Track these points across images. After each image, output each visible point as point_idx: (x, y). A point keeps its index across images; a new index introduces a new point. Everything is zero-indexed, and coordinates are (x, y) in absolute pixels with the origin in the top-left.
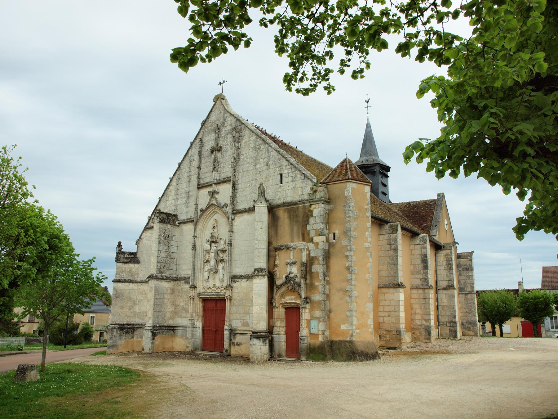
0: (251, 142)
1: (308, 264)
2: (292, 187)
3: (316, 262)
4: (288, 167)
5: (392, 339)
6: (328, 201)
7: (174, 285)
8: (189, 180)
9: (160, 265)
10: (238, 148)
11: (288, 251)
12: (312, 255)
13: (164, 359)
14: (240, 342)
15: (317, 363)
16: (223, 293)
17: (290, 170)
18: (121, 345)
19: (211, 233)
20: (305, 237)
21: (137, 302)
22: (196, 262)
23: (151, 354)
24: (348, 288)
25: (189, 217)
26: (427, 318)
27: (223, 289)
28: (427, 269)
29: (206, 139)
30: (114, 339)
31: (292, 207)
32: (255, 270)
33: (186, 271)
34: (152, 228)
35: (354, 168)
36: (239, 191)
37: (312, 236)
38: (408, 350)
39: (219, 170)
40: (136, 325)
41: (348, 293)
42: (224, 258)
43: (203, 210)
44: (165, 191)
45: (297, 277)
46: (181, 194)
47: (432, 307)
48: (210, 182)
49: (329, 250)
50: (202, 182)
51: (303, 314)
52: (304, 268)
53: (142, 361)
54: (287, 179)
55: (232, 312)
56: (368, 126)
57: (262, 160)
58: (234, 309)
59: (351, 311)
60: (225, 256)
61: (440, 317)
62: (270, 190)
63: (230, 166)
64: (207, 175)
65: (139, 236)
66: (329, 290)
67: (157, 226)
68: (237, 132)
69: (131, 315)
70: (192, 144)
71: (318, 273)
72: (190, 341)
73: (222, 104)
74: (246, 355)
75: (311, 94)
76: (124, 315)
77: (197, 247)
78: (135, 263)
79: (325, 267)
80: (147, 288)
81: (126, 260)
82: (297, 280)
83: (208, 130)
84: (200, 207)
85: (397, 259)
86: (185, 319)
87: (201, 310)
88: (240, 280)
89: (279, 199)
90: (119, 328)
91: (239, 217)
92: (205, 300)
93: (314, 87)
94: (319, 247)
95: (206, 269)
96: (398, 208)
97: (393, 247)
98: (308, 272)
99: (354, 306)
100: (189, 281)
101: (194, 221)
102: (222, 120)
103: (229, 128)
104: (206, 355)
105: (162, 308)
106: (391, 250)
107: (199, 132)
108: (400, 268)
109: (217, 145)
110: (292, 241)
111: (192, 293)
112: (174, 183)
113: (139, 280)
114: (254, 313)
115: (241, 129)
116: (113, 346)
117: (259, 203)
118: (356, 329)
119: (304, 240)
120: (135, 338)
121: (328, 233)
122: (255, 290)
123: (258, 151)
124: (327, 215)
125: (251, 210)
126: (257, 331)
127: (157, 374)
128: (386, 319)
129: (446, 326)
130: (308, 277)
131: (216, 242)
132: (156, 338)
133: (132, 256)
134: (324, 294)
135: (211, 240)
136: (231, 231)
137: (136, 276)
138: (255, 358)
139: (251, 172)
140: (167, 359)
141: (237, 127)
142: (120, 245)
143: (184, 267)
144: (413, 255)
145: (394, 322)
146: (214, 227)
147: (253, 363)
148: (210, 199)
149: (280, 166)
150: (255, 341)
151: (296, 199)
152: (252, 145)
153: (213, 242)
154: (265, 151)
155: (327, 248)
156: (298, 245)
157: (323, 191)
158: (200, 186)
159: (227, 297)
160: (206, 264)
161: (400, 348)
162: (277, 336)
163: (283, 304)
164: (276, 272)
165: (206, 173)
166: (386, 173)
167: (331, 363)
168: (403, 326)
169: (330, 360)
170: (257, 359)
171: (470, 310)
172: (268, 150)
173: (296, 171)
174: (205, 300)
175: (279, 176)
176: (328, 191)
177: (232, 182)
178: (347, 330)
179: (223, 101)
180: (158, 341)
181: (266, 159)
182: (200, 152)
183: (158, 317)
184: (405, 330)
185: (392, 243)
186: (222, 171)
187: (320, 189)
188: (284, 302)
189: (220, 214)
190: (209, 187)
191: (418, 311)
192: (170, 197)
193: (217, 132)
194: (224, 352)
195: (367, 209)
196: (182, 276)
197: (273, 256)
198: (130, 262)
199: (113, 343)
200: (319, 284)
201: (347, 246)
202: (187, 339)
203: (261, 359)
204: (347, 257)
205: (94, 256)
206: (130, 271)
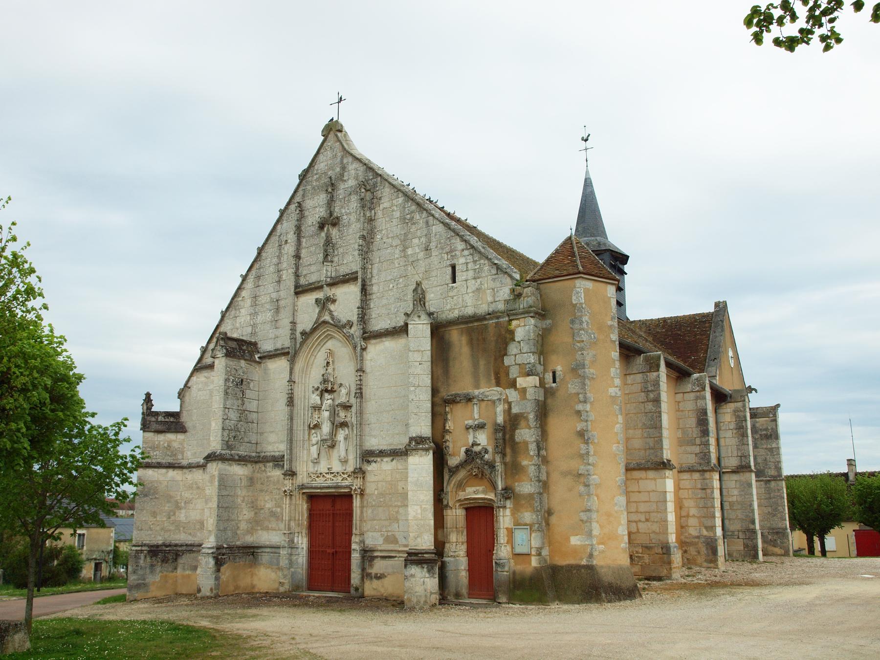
0: (395, 208)
1: (508, 428)
2: (474, 288)
3: (523, 423)
4: (466, 252)
5: (653, 562)
6: (542, 313)
7: (254, 471)
9: (229, 435)
10: (371, 220)
11: (470, 403)
12: (515, 410)
13: (244, 607)
14: (381, 572)
15: (530, 607)
16: (346, 483)
17: (470, 257)
18: (154, 583)
19: (323, 375)
20: (502, 378)
21: (183, 504)
22: (295, 428)
23: (215, 597)
24: (582, 469)
25: (279, 346)
26: (709, 524)
27: (346, 476)
28: (708, 435)
29: (309, 204)
30: (140, 572)
31: (476, 324)
32: (411, 439)
33: (275, 444)
34: (211, 367)
35: (587, 253)
36: (374, 296)
37: (515, 376)
38: (683, 581)
39: (336, 259)
40: (182, 546)
41: (582, 479)
43: (306, 333)
44: (233, 299)
45: (486, 452)
46: (262, 305)
47: (717, 504)
48: (319, 282)
49: (545, 402)
50: (303, 281)
51: (501, 518)
52: (501, 434)
53: (204, 612)
54: (465, 273)
55: (365, 518)
56: (588, 183)
57: (416, 241)
58: (369, 512)
59: (589, 510)
61: (727, 522)
62: (432, 295)
63: (356, 253)
64: (313, 268)
65: (184, 382)
66: (548, 474)
67: (221, 363)
68: (367, 191)
69: (172, 528)
70: (282, 213)
71: (526, 443)
72: (286, 572)
73: (339, 141)
74: (393, 596)
75: (801, 48)
76: (158, 528)
77: (295, 401)
78: (177, 431)
79: (540, 433)
80: (200, 477)
81: (160, 427)
82: (486, 456)
83: (314, 188)
84: (300, 328)
85: (660, 417)
86: (274, 532)
87: (306, 515)
88: (379, 459)
89: (450, 310)
90: (149, 552)
91: (375, 344)
92: (313, 499)
93: (805, 34)
94: (528, 396)
95: (314, 440)
96: (644, 330)
97: (652, 396)
98: (507, 442)
99: (594, 502)
100: (281, 463)
101: (289, 354)
102: (338, 169)
103: (352, 183)
104: (318, 597)
105: (233, 514)
106: (648, 401)
107: (296, 192)
108: (665, 433)
109: (331, 214)
110: (477, 387)
111: (288, 485)
112: (249, 284)
113: (185, 462)
114: (410, 518)
115: (375, 186)
116: (138, 587)
117: (416, 319)
118: (599, 544)
119: (498, 384)
120: (179, 571)
121: (542, 371)
122: (412, 476)
123: (409, 224)
124: (540, 338)
125: (402, 330)
126: (416, 551)
127: (245, 633)
128: (641, 525)
129: (738, 538)
130: (508, 450)
131: (331, 391)
132: (223, 569)
133: (172, 419)
134: (539, 481)
135: (322, 387)
136: (361, 370)
137: (180, 457)
138: (414, 600)
139: (396, 262)
140: (249, 607)
141: (367, 181)
142: (148, 399)
143: (272, 438)
144: (682, 411)
145: (658, 531)
146: (328, 363)
147: (412, 609)
148: (320, 312)
149: (451, 251)
150: (414, 570)
151: (483, 309)
152: (397, 214)
153: (327, 391)
154: (421, 223)
155: (542, 398)
156: (488, 393)
157: (533, 294)
158: (300, 289)
159: (355, 490)
160: (313, 431)
161: (669, 577)
162: (452, 559)
163: (462, 501)
164: (447, 444)
165: (310, 265)
166: (621, 266)
167: (554, 606)
168: (672, 539)
169: (553, 601)
170: (418, 602)
171: (776, 510)
172: (427, 223)
173: (480, 259)
174: (313, 499)
175: (450, 268)
176: (541, 296)
177: (360, 280)
178: (581, 546)
179: (339, 134)
181: (423, 239)
182: (298, 230)
183: (225, 529)
184: (677, 545)
185: (650, 389)
186: (341, 262)
187: (528, 291)
188: (463, 498)
189: (338, 339)
190: (317, 291)
191: (693, 511)
192: (243, 311)
193: (330, 190)
194: (352, 591)
195: (611, 326)
196: (268, 454)
197: (441, 415)
198: (168, 431)
199: (139, 579)
200: (528, 462)
201: (578, 394)
202: (280, 569)
203: (426, 602)
204: (579, 413)
205: (125, 416)
206: (168, 446)
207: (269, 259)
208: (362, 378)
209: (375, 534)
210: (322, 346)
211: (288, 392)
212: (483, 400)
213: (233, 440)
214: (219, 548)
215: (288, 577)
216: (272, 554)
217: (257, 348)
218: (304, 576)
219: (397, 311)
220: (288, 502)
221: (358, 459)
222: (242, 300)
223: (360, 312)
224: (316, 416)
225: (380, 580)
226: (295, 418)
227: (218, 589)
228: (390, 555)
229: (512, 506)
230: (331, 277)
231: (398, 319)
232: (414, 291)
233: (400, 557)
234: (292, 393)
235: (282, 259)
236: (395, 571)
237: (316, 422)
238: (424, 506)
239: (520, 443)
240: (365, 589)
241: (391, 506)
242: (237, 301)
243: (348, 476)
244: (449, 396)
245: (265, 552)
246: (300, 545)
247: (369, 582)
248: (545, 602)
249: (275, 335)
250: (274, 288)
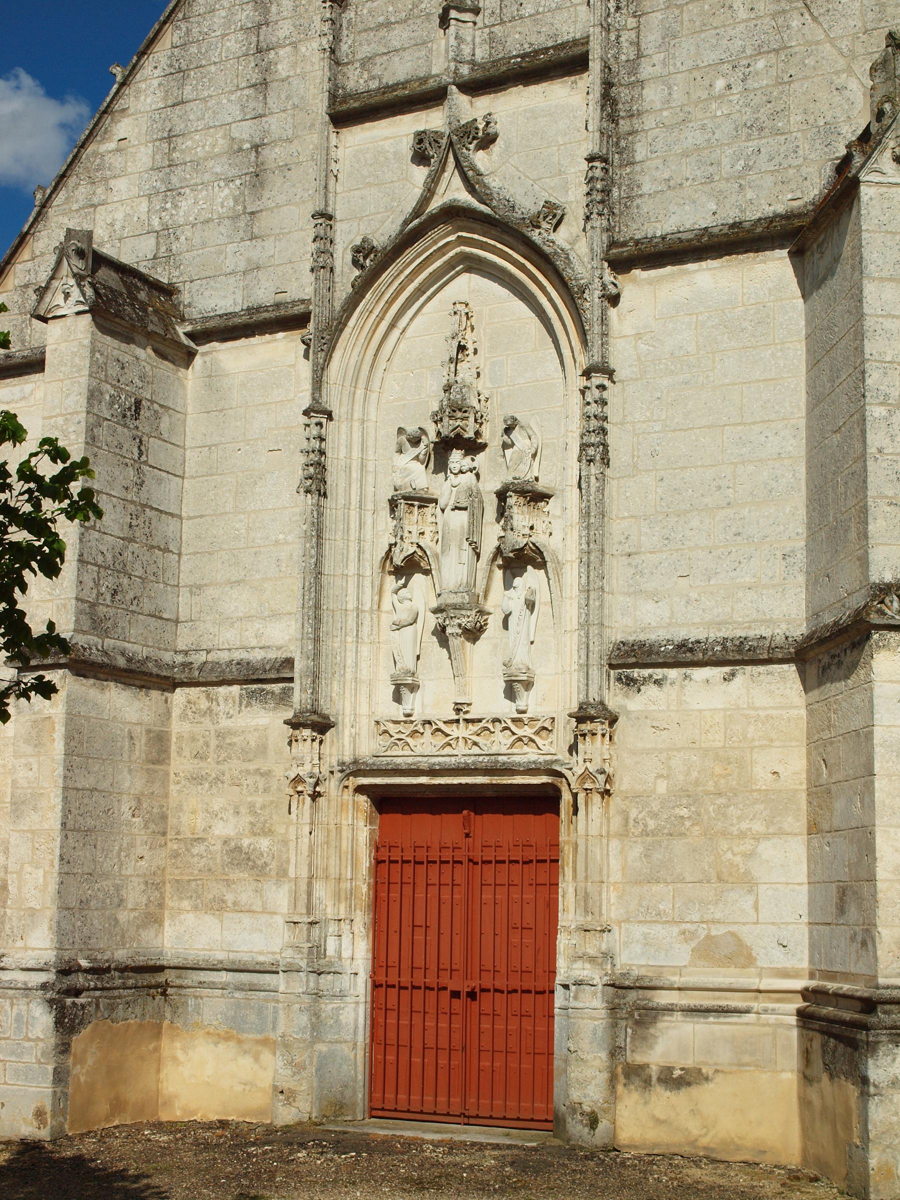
8: (255, 78)
9: (97, 584)
14: (689, 1063)
19: (448, 388)
27: (527, 731)
36: (649, 122)
42: (539, 538)
48: (424, 80)
60: (539, 526)
64: (398, 36)
74: (738, 1148)
86: (246, 919)
87: (365, 861)
100: (277, 687)
132: (78, 1041)
146: (461, 348)
165: (388, 25)
177: (595, 66)
180: (90, 1062)
192: (120, 185)
196: (224, 657)
207: (223, 13)
208: (605, 394)
209: (658, 931)
210: (430, 298)
211: (305, 445)
213: (108, 602)
214: (66, 970)
215: (304, 1074)
216: (237, 995)
217: (175, 307)
218: (360, 1068)
219: (748, 167)
220: (307, 818)
221: (594, 672)
222: (118, 150)
223: (598, 173)
224: (415, 530)
225: (684, 1091)
226: (326, 535)
227: (63, 1113)
228: (723, 1003)
230: (473, 63)
231: (750, 194)
232: (873, 69)
233: (766, 1011)
234: (322, 453)
235: (274, 9)
236: (746, 1059)
237: (414, 548)
240: (620, 1121)
241: (724, 834)
242: (95, 154)
243: (537, 733)
245: (212, 986)
246: (346, 963)
247: (635, 1096)
249: (249, 260)
250: (243, 107)
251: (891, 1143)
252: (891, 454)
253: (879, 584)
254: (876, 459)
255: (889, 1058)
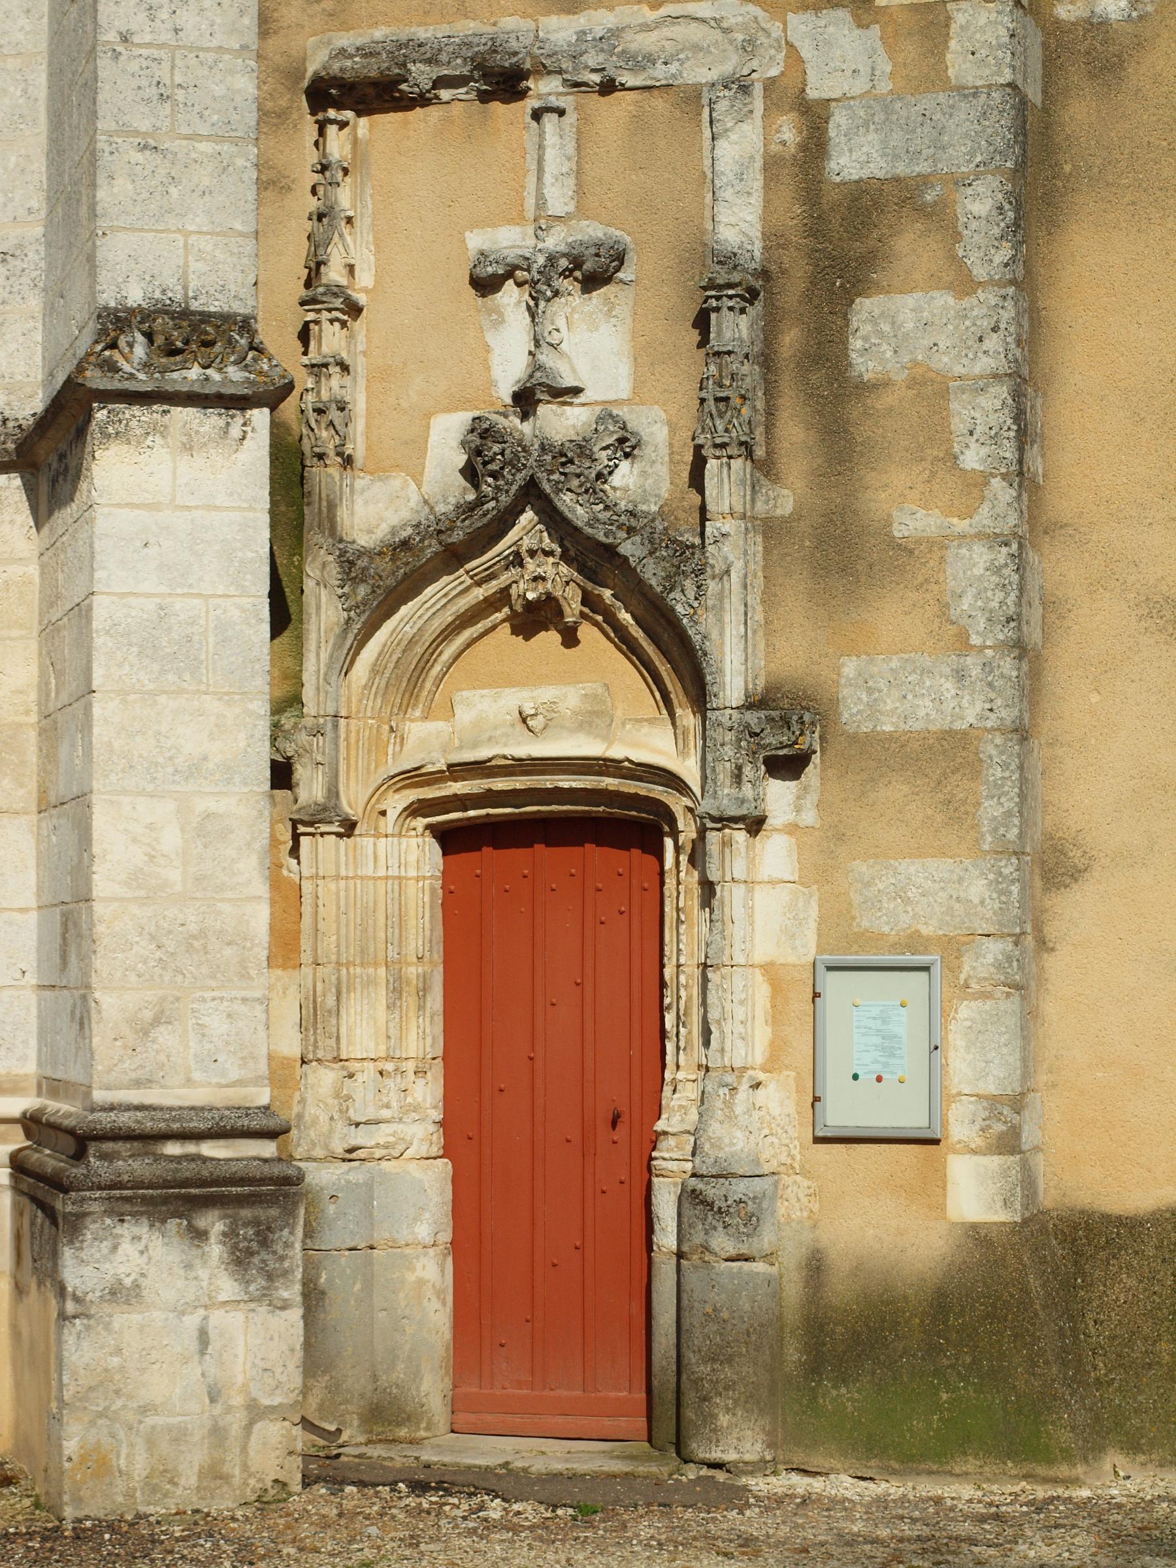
82: (625, 476)
212: (608, 87)
229: (809, 817)
238: (202, 805)
239: (881, 385)
244: (342, 53)
248: (1051, 1462)
251: (106, 1408)
252: (149, 45)
253: (116, 310)
254: (116, 55)
255: (105, 1246)
